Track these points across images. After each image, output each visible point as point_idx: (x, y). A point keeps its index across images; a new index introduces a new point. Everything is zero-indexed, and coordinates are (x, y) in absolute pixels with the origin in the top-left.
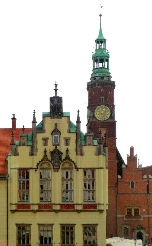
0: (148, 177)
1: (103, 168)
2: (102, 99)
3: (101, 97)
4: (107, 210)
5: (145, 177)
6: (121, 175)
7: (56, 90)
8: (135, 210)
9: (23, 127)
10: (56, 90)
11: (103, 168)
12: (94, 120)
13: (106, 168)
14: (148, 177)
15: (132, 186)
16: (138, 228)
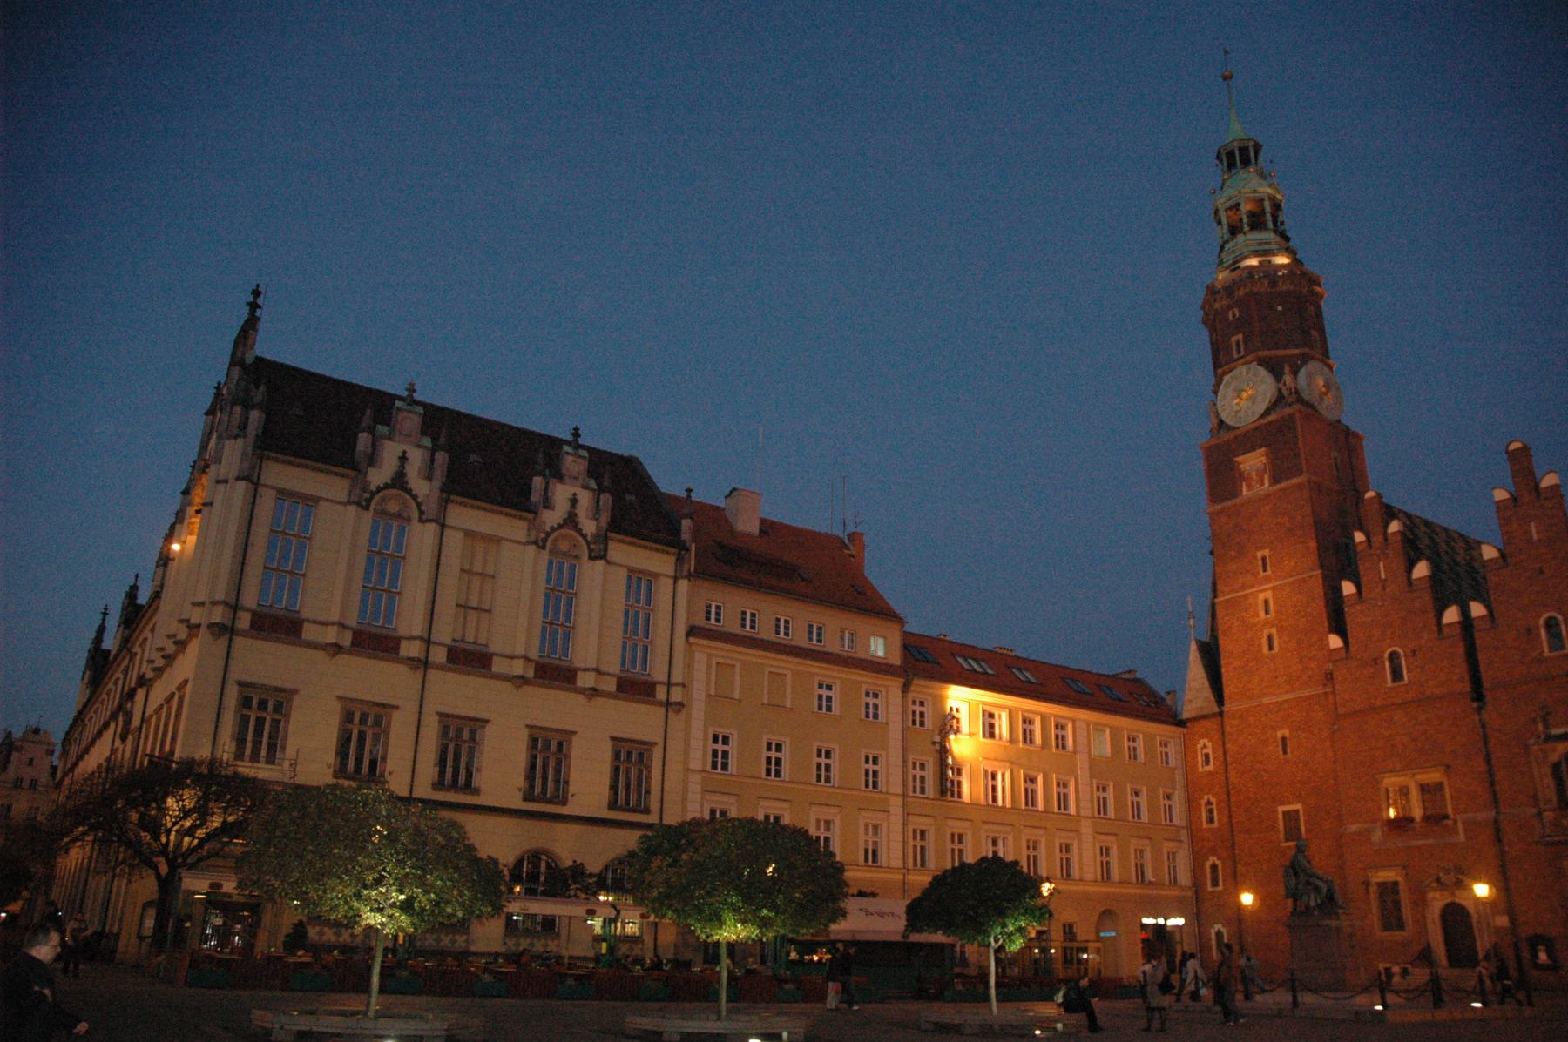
0: (1465, 612)
1: (226, 481)
2: (1238, 343)
3: (1234, 339)
4: (211, 626)
5: (1451, 615)
6: (1342, 632)
7: (254, 306)
8: (1424, 789)
9: (684, 495)
10: (254, 306)
11: (226, 481)
12: (1226, 436)
13: (238, 478)
14: (1465, 612)
15: (1397, 675)
16: (1438, 880)
